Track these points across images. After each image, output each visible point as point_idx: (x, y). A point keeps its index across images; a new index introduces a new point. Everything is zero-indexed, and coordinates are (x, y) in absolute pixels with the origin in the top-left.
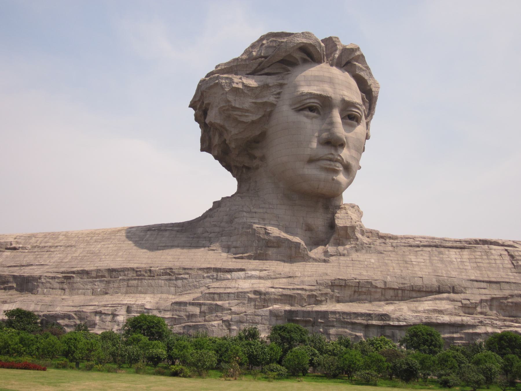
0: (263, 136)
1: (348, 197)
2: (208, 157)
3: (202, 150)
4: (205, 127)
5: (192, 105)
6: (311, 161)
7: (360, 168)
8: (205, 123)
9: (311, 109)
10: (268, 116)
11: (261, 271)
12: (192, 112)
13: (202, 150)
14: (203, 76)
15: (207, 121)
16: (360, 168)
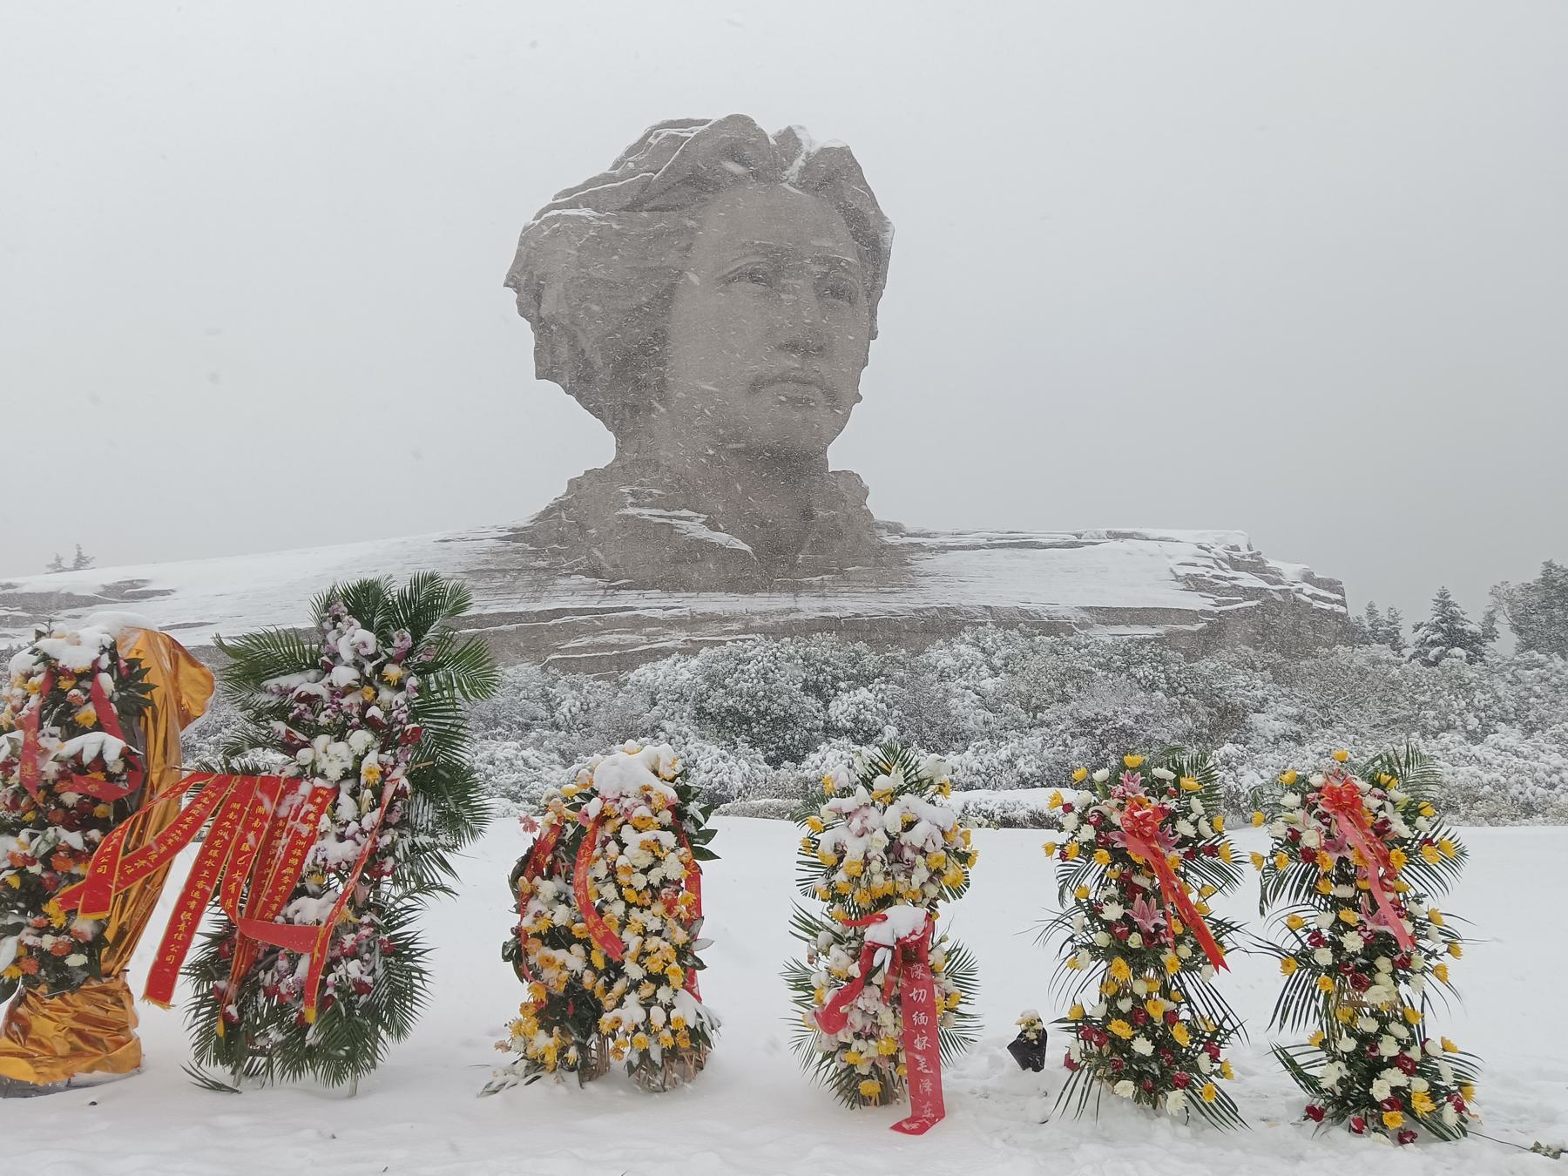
0: (661, 337)
1: (838, 456)
2: (553, 389)
3: (538, 377)
4: (541, 326)
5: (512, 282)
6: (756, 386)
7: (859, 398)
8: (541, 319)
9: (753, 277)
10: (666, 297)
11: (665, 609)
12: (512, 295)
13: (538, 377)
14: (528, 219)
15: (544, 313)
16: (859, 398)
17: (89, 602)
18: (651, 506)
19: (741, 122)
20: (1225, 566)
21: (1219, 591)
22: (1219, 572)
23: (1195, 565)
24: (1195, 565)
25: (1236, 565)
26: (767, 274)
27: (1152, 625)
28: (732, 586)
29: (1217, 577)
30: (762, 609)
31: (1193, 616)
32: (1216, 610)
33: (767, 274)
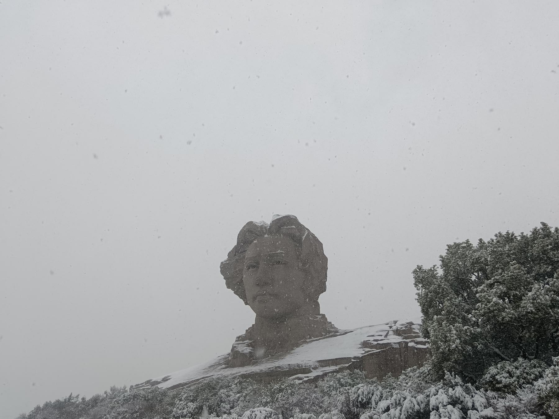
9: (254, 267)
17: (160, 383)
18: (240, 341)
19: (250, 223)
20: (391, 333)
21: (372, 347)
22: (382, 338)
23: (373, 336)
24: (373, 336)
25: (398, 332)
26: (254, 266)
27: (336, 365)
28: (242, 365)
29: (374, 340)
30: (234, 372)
31: (347, 360)
32: (361, 356)
33: (254, 266)
